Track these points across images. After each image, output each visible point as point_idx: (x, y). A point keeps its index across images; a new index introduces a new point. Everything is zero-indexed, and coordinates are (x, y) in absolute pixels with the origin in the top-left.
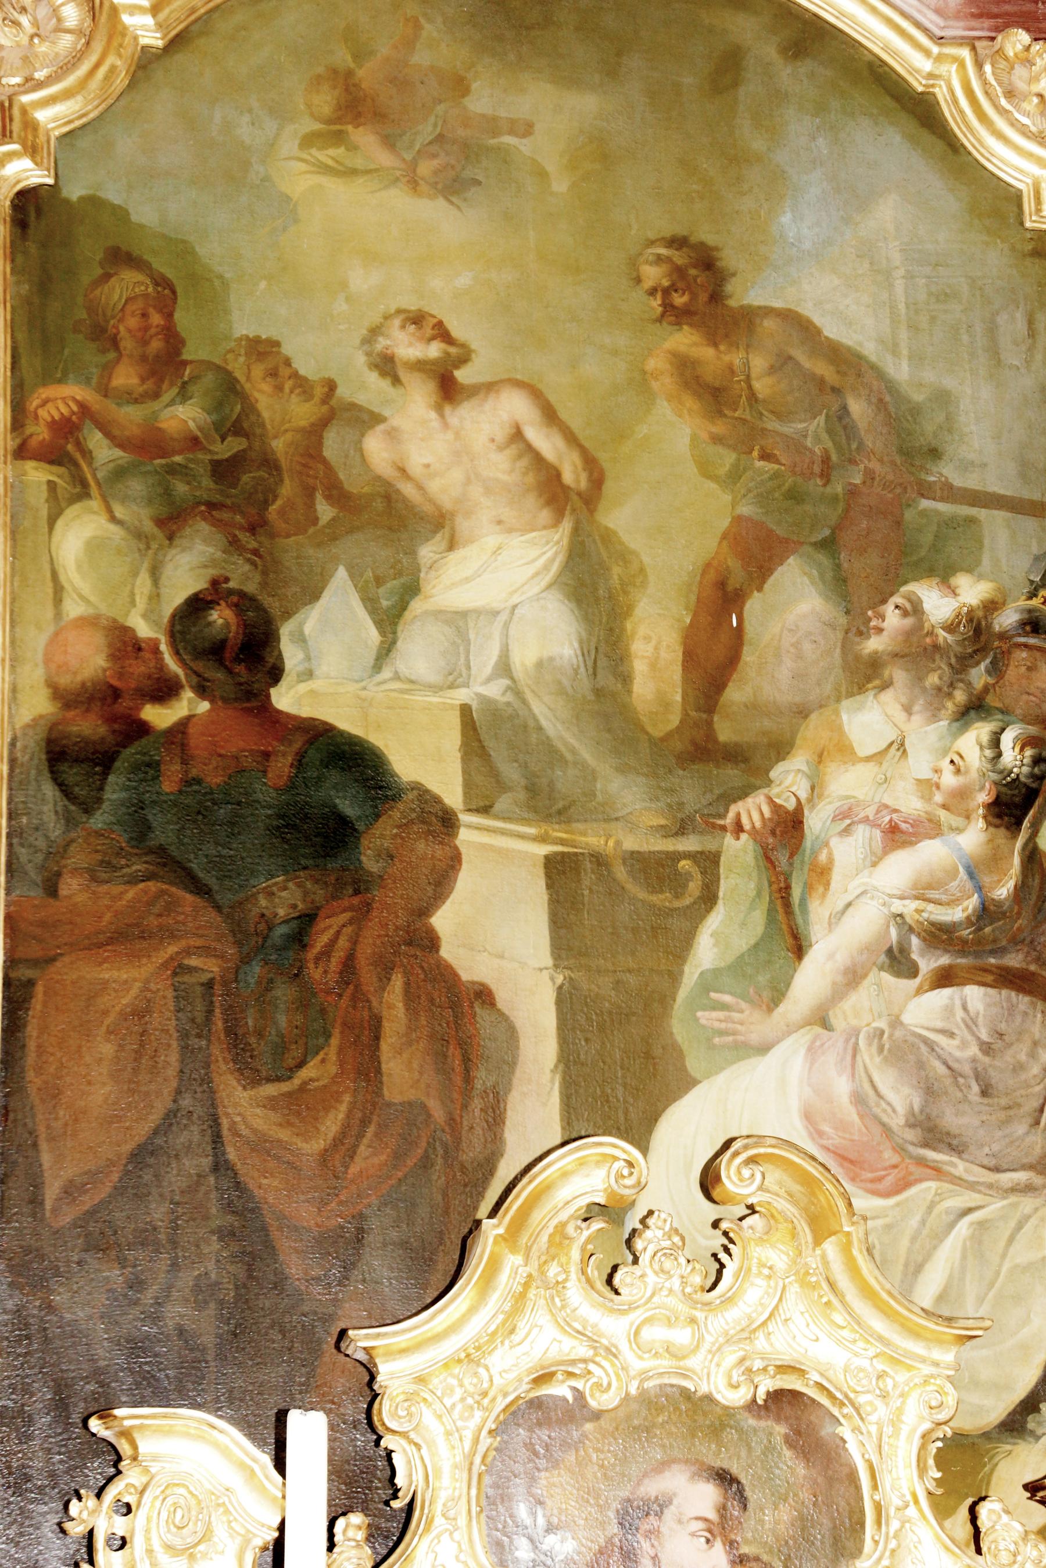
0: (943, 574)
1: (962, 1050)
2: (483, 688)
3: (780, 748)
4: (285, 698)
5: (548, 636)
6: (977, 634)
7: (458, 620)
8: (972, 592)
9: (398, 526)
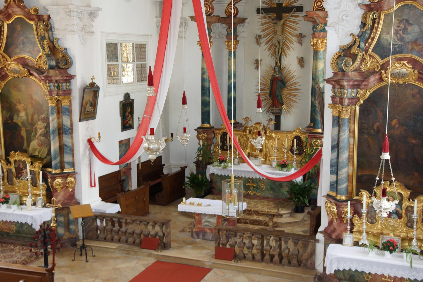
0: (43, 114)
1: (43, 140)
2: (22, 120)
3: (35, 124)
4: (14, 121)
5: (25, 118)
6: (44, 117)
7: (21, 117)
8: (44, 116)
9: (18, 111)
